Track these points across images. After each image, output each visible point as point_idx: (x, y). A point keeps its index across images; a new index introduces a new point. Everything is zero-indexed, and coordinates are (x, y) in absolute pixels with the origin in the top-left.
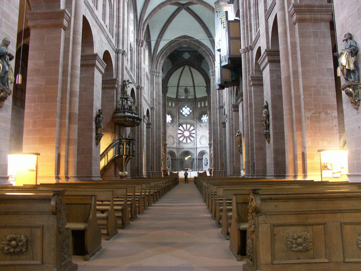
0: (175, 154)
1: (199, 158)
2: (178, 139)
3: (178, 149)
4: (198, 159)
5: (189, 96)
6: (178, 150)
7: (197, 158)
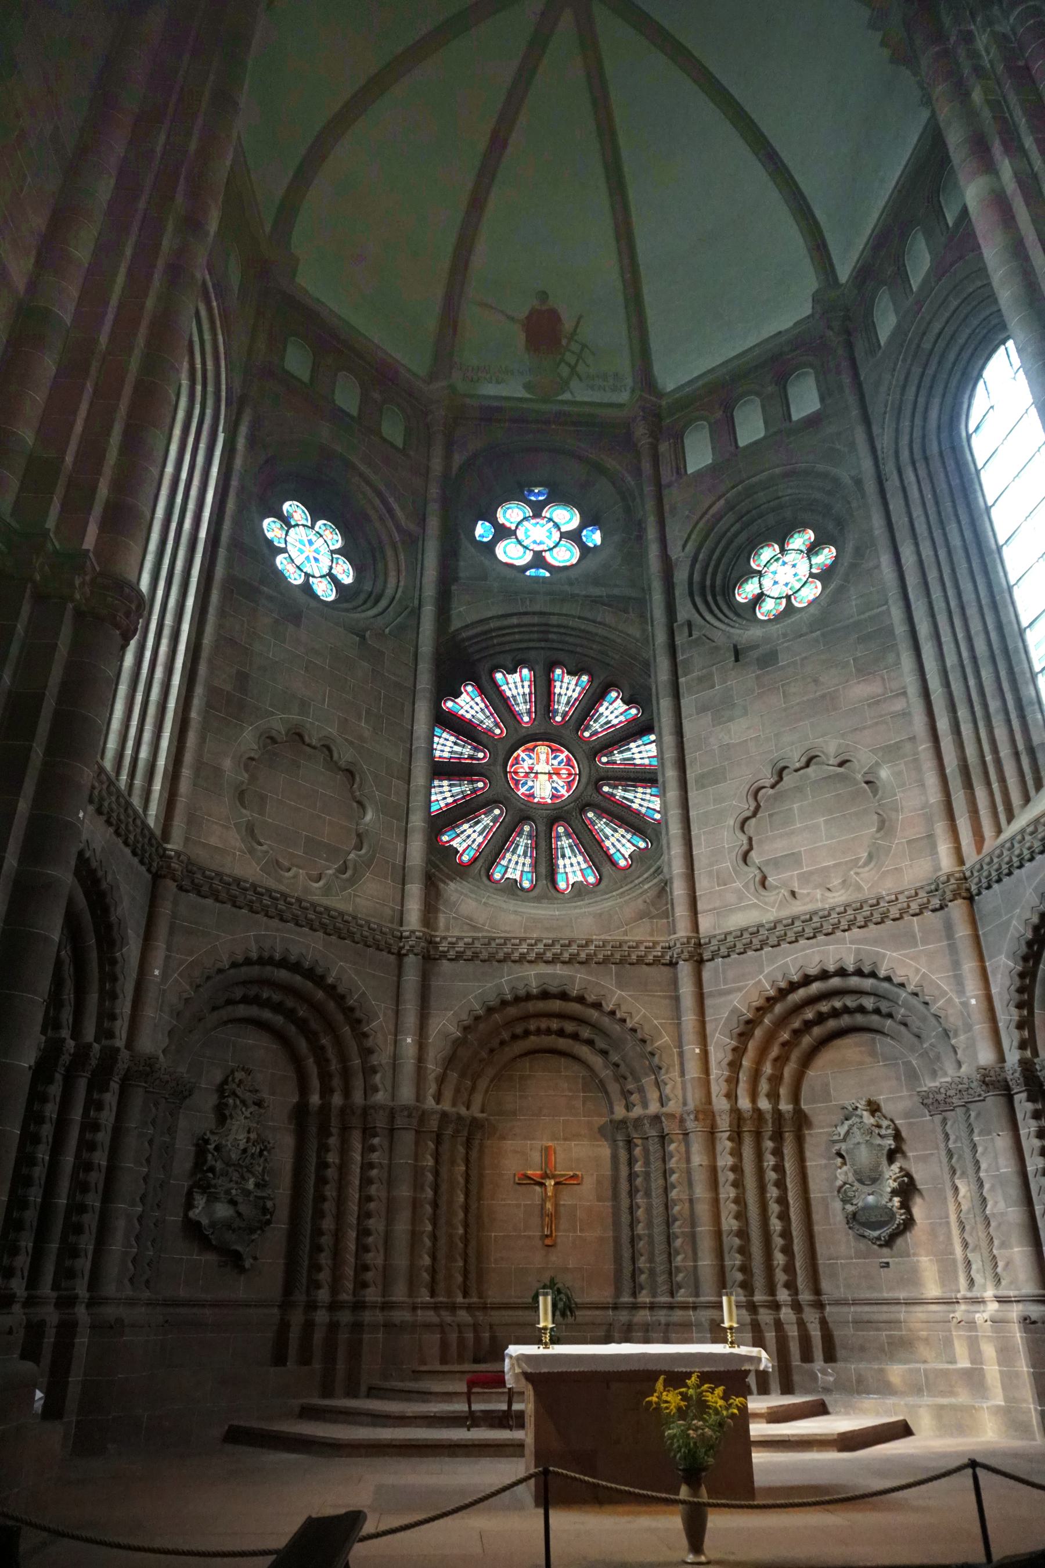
0: (356, 1024)
1: (744, 1103)
2: (417, 821)
3: (410, 960)
4: (736, 1113)
5: (574, 383)
6: (411, 978)
7: (721, 1104)
